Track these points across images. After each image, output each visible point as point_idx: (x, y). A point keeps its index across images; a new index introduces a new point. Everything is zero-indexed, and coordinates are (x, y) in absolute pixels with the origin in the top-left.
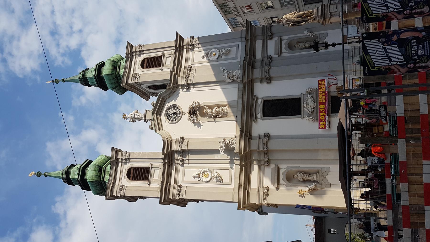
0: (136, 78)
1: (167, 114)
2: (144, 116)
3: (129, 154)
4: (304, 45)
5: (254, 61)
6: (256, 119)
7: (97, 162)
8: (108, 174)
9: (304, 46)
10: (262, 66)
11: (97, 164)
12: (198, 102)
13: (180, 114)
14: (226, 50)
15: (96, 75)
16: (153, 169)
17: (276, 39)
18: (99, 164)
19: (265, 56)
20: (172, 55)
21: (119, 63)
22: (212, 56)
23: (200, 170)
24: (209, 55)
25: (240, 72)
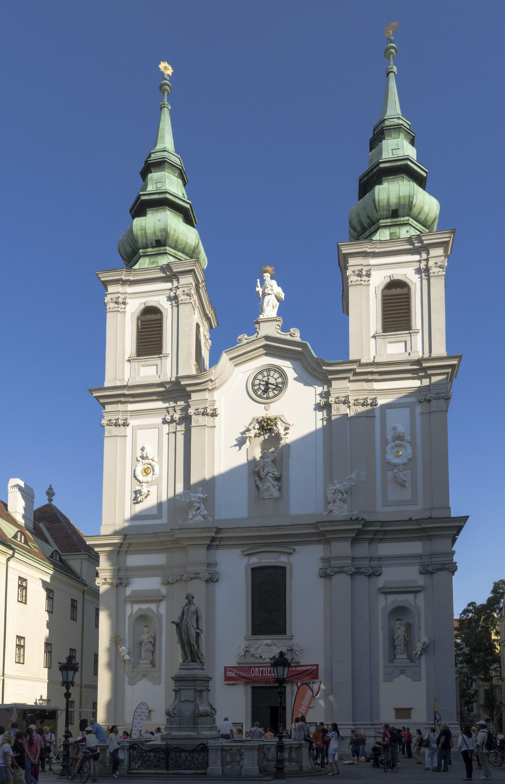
0: (360, 275)
1: (268, 369)
2: (267, 317)
3: (187, 301)
4: (398, 637)
5: (371, 541)
6: (248, 555)
7: (175, 231)
8: (153, 263)
9: (395, 637)
10: (353, 559)
11: (169, 231)
12: (287, 433)
13: (268, 399)
14: (405, 479)
15: (382, 165)
16: (158, 362)
17: (421, 580)
18: (171, 236)
19: (383, 563)
20: (409, 354)
21: (408, 220)
22: (395, 450)
23: (156, 459)
24: (398, 442)
25: (341, 514)
